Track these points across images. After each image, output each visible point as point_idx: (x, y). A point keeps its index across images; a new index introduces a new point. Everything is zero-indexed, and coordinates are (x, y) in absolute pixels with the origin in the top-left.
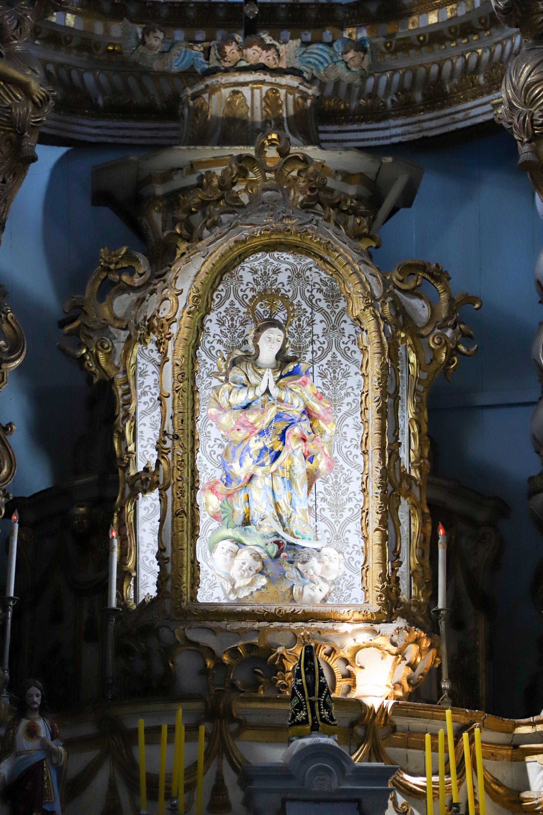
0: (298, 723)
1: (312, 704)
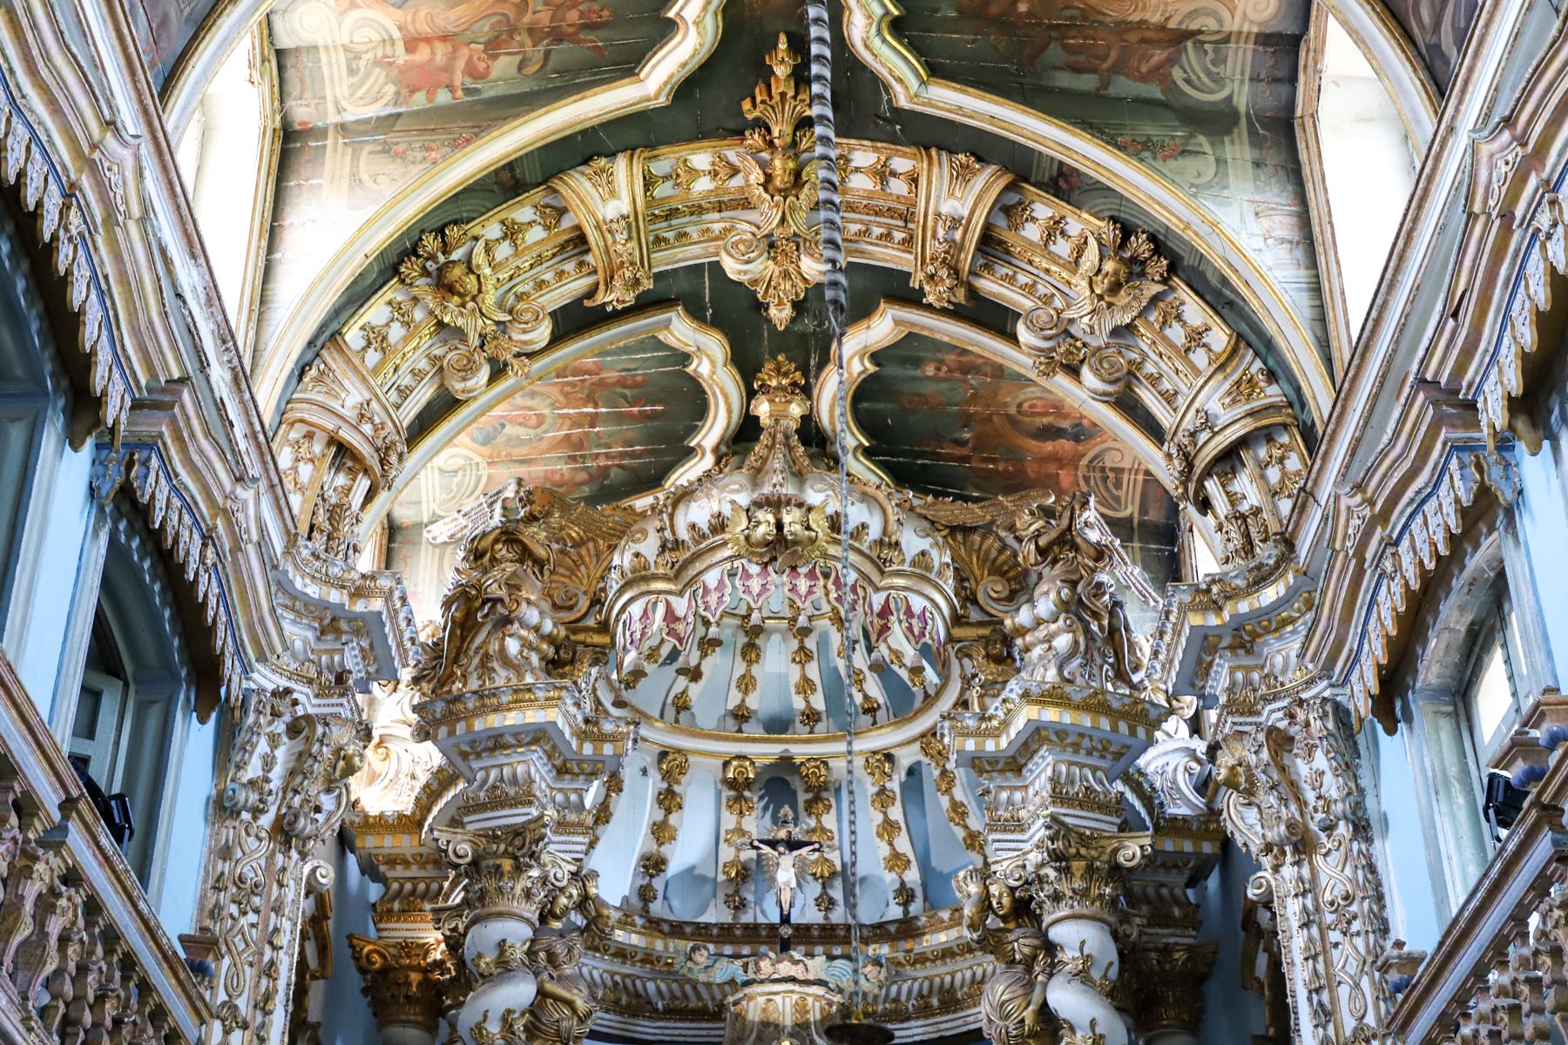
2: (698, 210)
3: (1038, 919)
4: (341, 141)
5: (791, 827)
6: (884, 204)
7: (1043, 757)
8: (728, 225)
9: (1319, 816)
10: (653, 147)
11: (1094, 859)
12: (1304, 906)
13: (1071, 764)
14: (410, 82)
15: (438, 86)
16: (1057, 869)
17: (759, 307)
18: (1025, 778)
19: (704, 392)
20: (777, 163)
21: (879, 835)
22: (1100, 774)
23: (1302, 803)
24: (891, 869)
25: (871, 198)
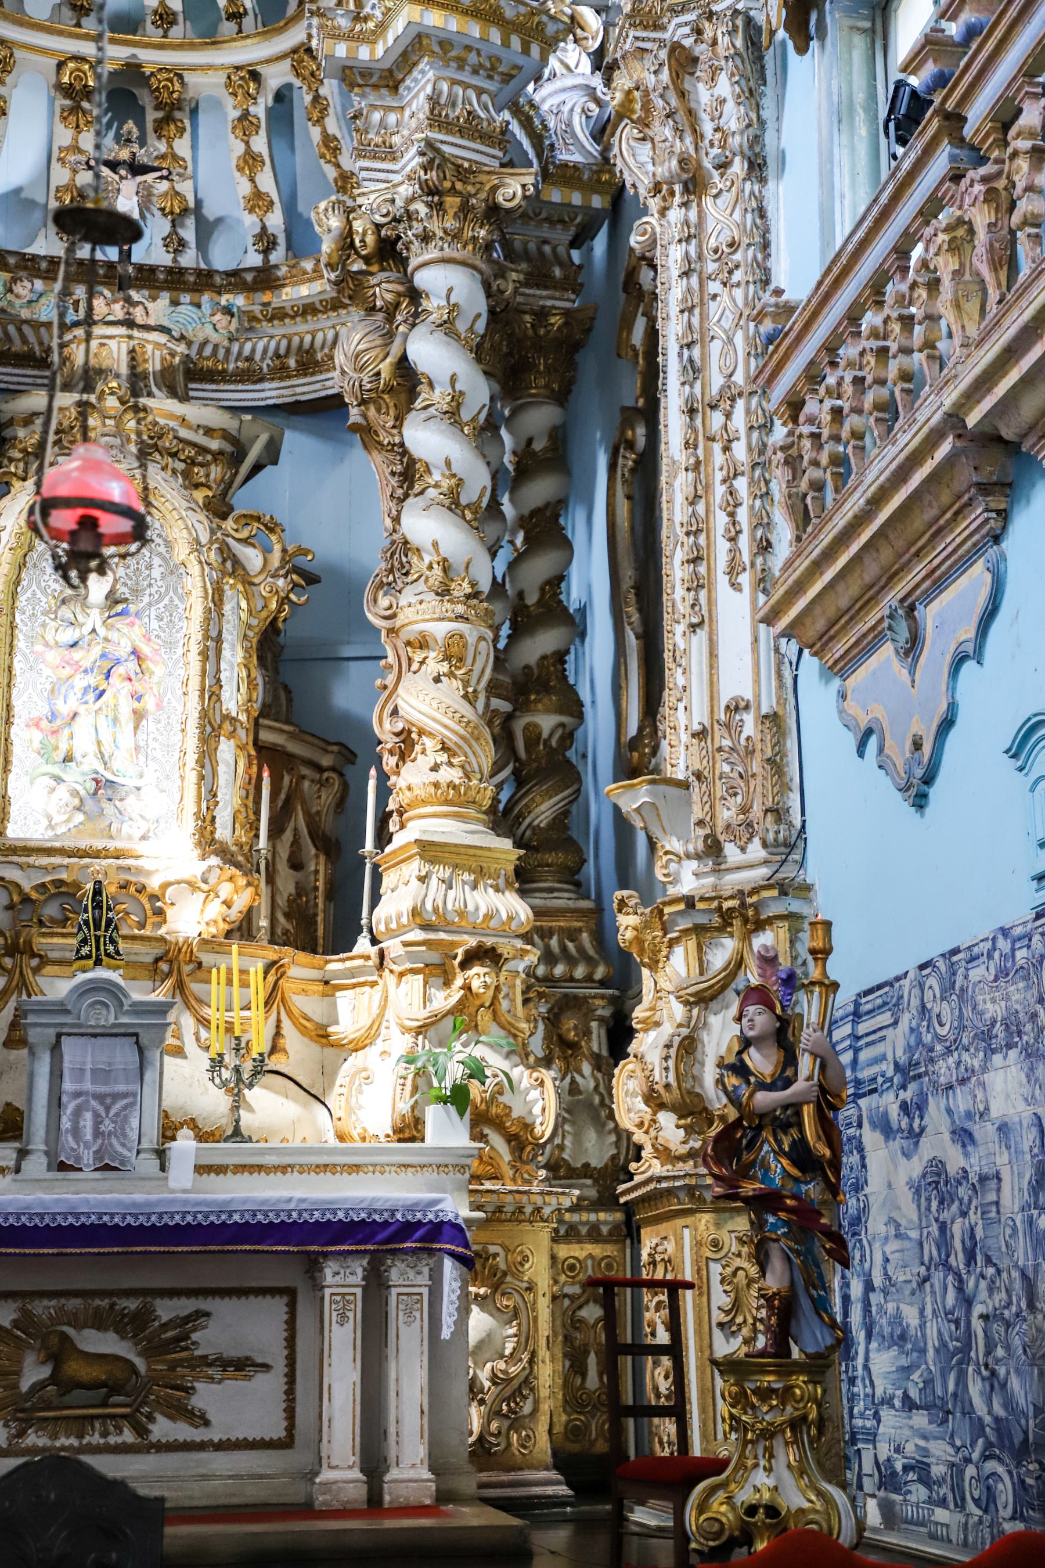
0: (82, 958)
1: (97, 939)
3: (404, 262)
5: (135, 147)
7: (423, 72)
9: (715, 151)
11: (470, 195)
12: (687, 253)
13: (454, 82)
16: (429, 205)
18: (402, 98)
21: (240, 169)
22: (485, 97)
23: (698, 135)
24: (251, 210)
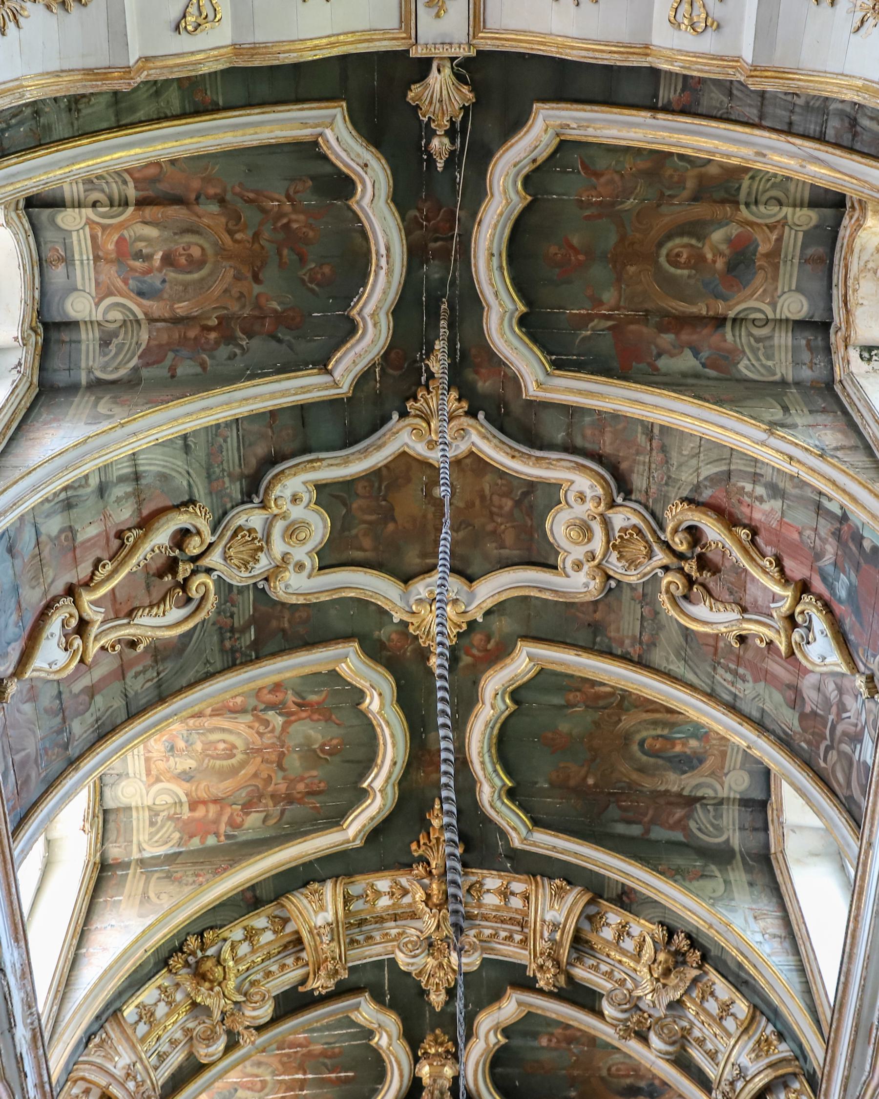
2: (380, 920)
4: (139, 871)
6: (506, 915)
8: (400, 930)
10: (349, 875)
14: (189, 830)
15: (208, 833)
17: (423, 993)
19: (383, 1061)
20: (434, 886)
25: (498, 911)
